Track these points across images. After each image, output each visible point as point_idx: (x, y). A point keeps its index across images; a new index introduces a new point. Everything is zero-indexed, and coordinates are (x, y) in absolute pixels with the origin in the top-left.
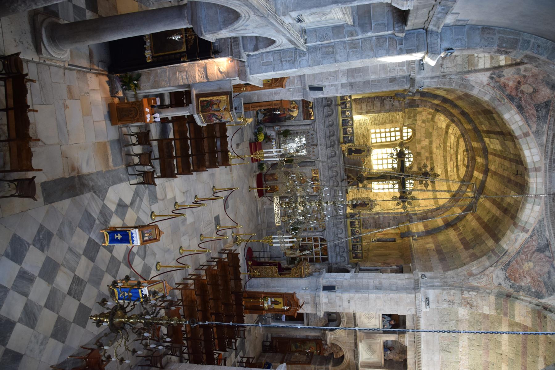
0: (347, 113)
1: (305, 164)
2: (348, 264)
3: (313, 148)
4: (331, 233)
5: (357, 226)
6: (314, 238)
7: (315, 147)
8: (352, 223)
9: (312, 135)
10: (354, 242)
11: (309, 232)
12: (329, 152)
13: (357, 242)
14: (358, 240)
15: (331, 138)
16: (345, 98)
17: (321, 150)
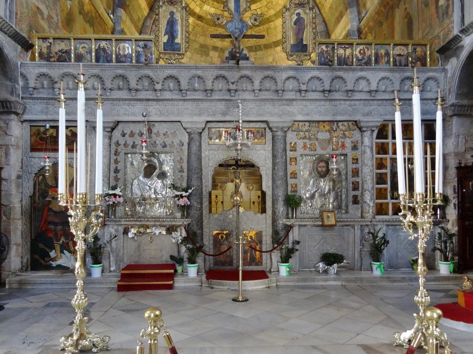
0: (81, 51)
1: (193, 158)
2: (444, 70)
3: (158, 134)
4: (367, 109)
5: (348, 51)
6: (378, 153)
7: (154, 130)
8: (343, 62)
9: (124, 135)
10: (388, 62)
11: (363, 164)
12: (167, 95)
13: (387, 54)
14: (383, 52)
15: (133, 84)
16: (45, 51)
17: (162, 114)
